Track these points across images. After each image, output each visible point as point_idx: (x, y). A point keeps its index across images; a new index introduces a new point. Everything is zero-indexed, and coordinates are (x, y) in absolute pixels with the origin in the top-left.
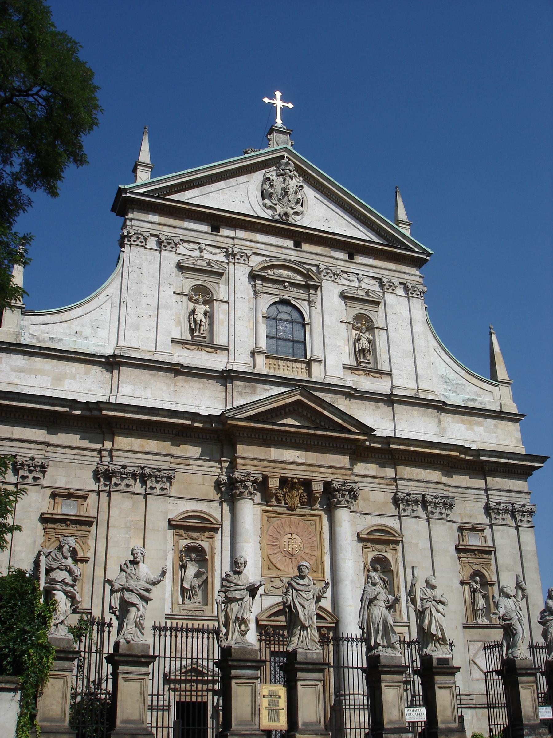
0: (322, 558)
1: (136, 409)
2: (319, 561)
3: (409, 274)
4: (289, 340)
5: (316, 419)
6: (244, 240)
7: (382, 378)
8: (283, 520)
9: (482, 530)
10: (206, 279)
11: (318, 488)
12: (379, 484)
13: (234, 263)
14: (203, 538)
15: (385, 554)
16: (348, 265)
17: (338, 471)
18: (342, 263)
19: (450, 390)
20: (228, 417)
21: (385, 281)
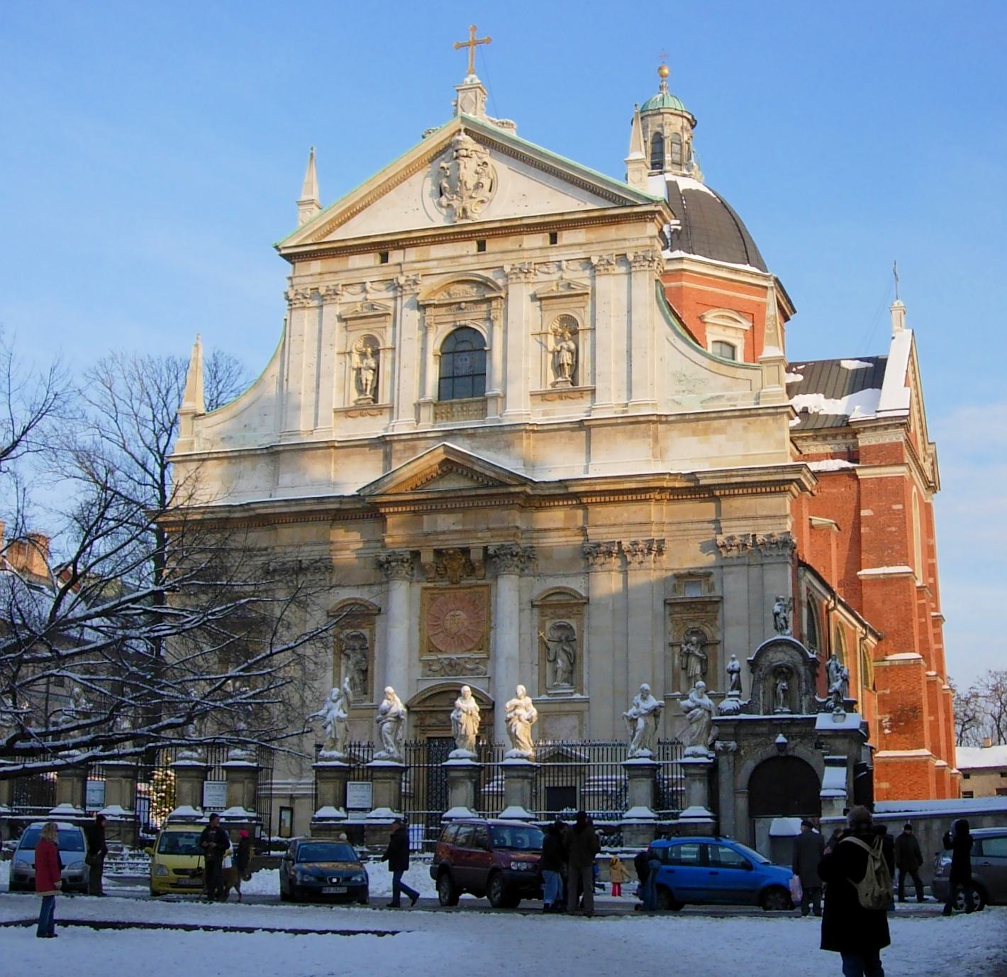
0: (488, 633)
1: (284, 503)
2: (485, 638)
3: (633, 239)
4: (470, 375)
5: (472, 477)
6: (413, 262)
7: (582, 397)
8: (447, 596)
9: (709, 575)
10: (372, 326)
11: (476, 555)
12: (565, 536)
13: (401, 296)
14: (364, 625)
15: (568, 621)
16: (545, 253)
17: (499, 533)
18: (538, 253)
19: (684, 391)
20: (364, 496)
21: (595, 260)
